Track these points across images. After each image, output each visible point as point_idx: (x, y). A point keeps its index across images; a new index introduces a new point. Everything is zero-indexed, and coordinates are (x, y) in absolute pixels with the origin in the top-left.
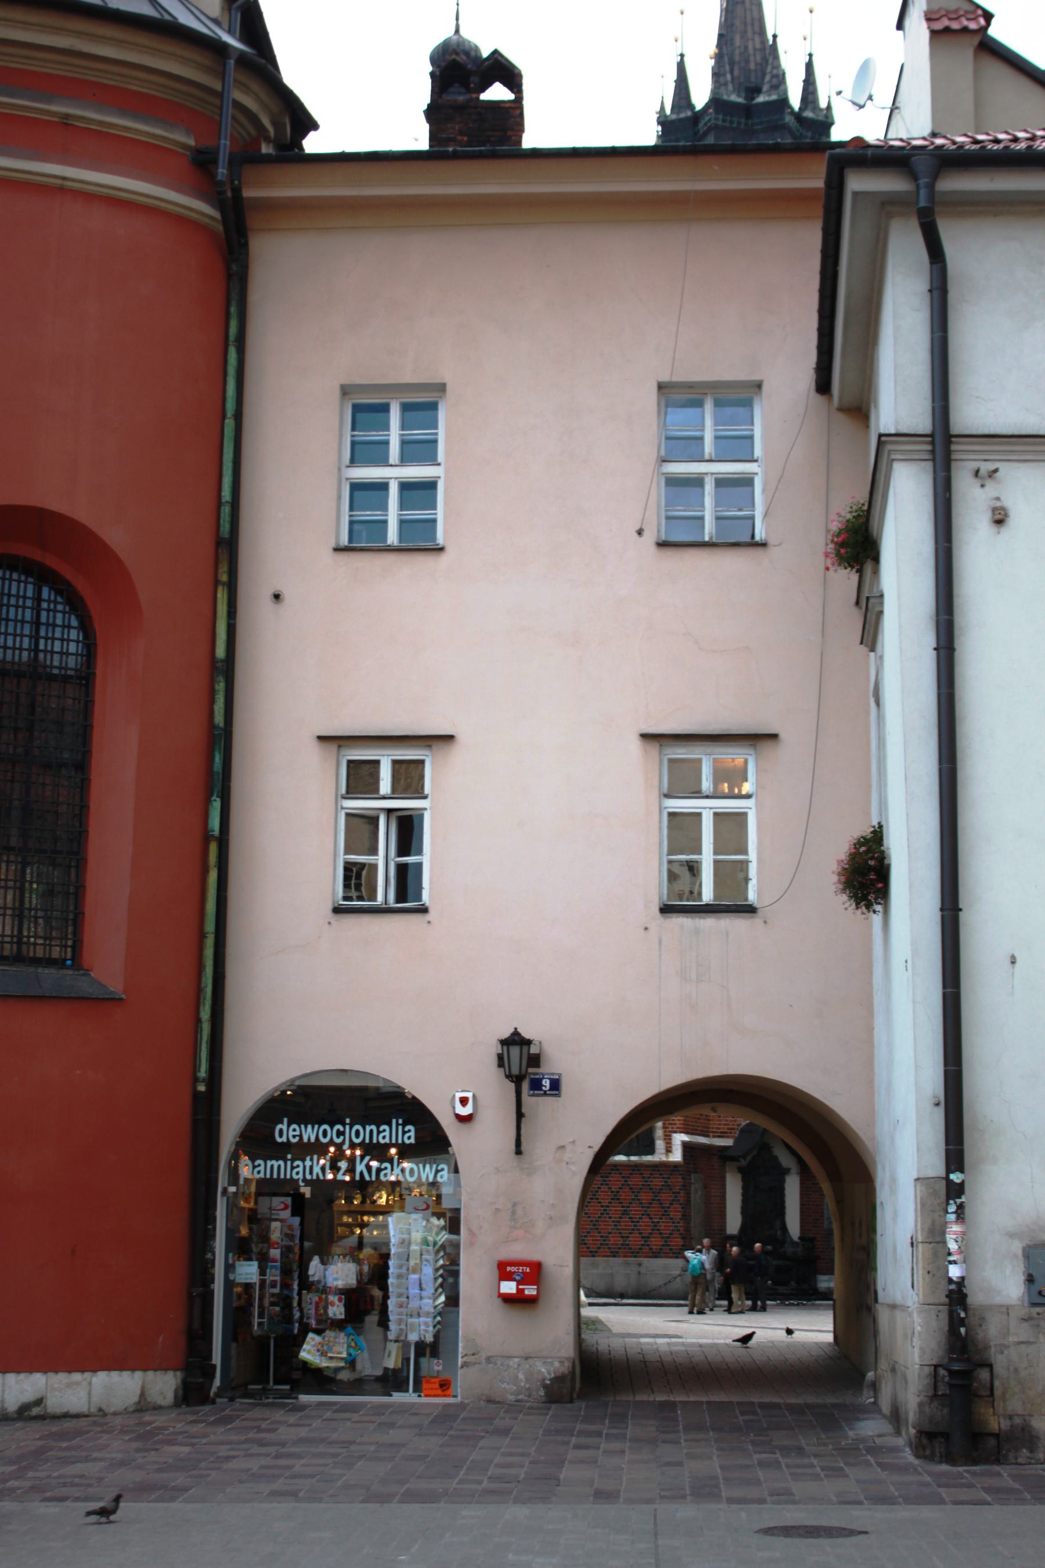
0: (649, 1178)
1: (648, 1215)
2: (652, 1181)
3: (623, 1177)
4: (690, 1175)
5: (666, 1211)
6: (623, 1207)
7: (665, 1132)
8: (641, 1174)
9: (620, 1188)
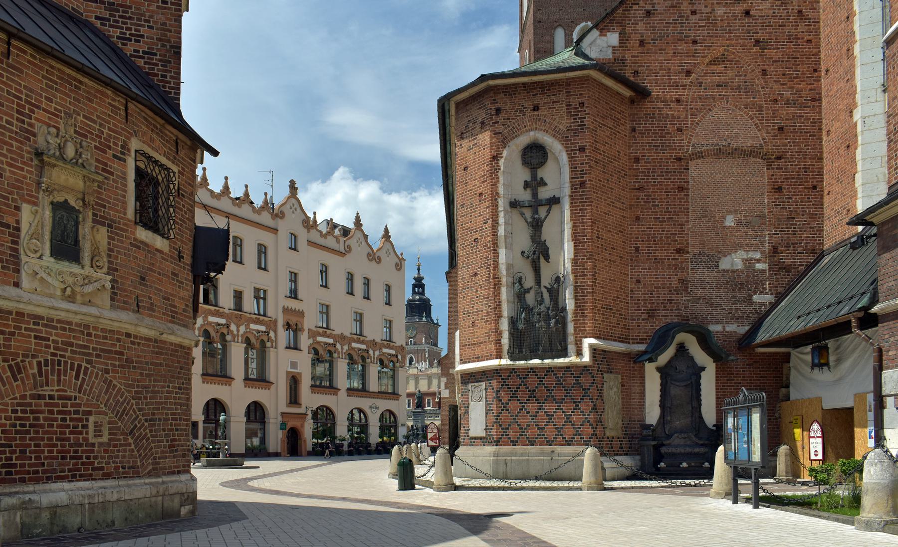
0: (561, 377)
1: (562, 409)
2: (564, 381)
3: (538, 378)
4: (602, 374)
5: (578, 406)
6: (538, 403)
7: (576, 337)
8: (556, 374)
9: (536, 387)
